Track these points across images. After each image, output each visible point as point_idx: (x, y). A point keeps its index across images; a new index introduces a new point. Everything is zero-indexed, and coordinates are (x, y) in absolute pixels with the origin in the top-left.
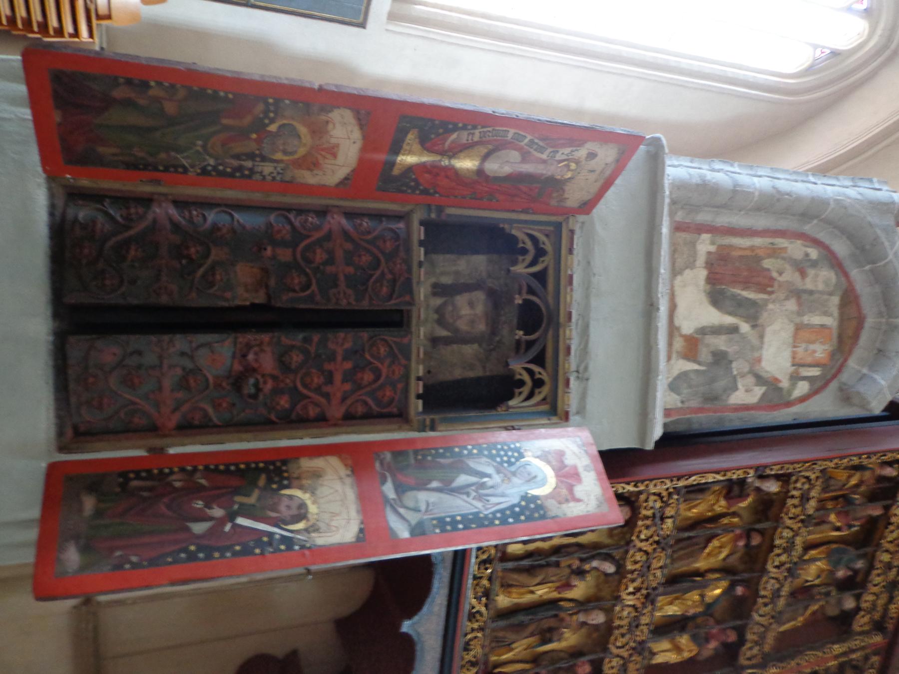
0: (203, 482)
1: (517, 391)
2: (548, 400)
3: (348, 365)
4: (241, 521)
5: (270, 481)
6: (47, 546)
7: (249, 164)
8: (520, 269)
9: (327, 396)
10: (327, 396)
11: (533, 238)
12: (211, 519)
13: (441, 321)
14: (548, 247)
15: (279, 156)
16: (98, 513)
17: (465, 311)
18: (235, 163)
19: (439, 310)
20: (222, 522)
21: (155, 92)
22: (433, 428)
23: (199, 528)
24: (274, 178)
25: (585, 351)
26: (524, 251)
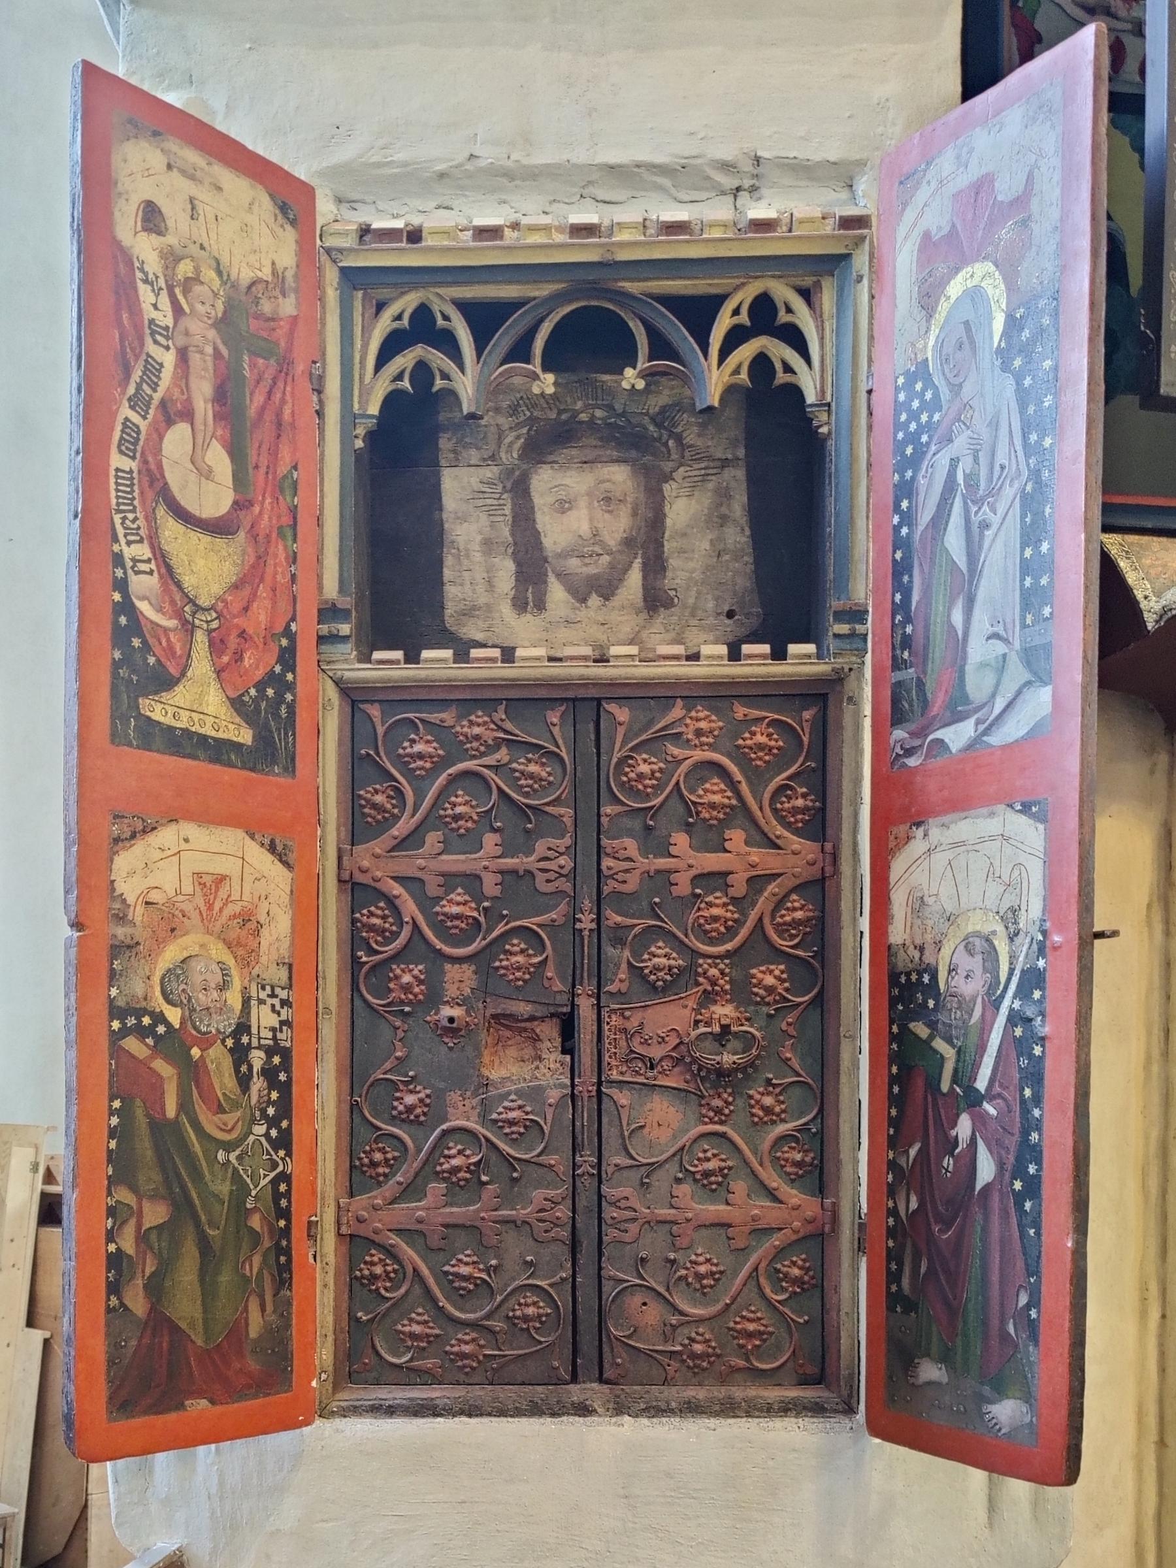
0: (913, 1152)
1: (781, 377)
2: (808, 281)
3: (681, 840)
4: (981, 1084)
5: (921, 1013)
6: (997, 1458)
7: (257, 1058)
8: (466, 384)
9: (757, 882)
10: (757, 882)
11: (392, 346)
12: (973, 1143)
13: (606, 587)
14: (408, 302)
15: (234, 999)
16: (945, 1358)
17: (580, 522)
18: (258, 1084)
19: (580, 592)
20: (980, 1120)
21: (128, 1243)
22: (857, 615)
23: (986, 1170)
24: (285, 1003)
25: (677, 175)
26: (422, 370)
